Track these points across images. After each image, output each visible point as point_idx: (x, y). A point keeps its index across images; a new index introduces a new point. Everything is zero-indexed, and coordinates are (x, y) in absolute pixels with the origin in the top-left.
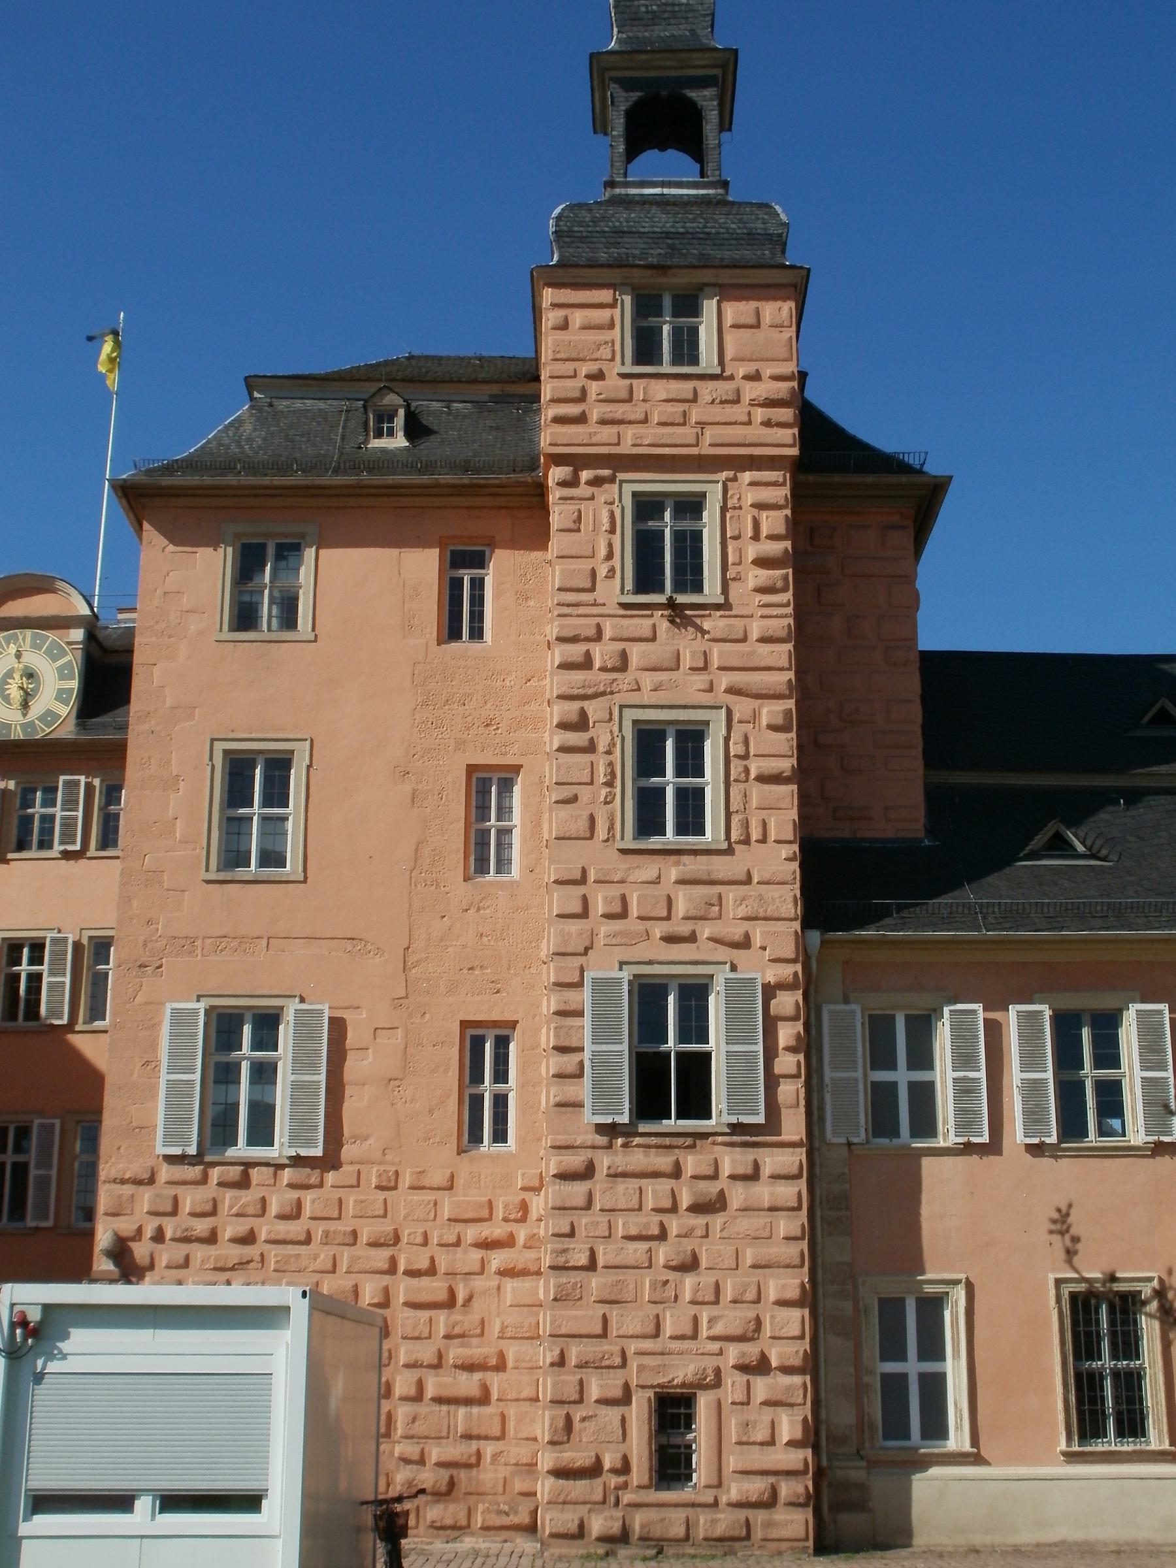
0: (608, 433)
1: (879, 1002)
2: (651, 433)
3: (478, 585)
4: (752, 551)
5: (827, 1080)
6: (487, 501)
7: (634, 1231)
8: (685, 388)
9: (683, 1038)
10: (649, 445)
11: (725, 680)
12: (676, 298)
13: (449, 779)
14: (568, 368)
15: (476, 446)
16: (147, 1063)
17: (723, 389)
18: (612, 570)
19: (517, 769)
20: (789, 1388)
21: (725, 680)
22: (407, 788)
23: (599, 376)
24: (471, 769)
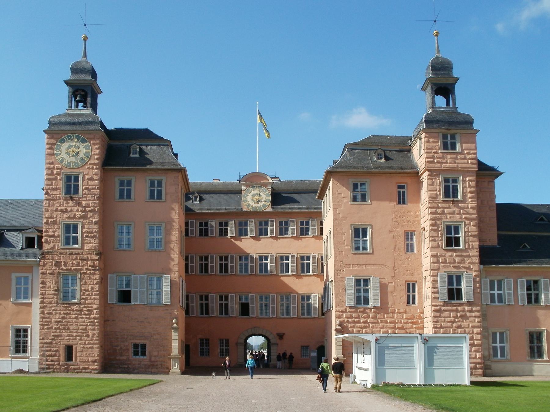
0: (438, 165)
1: (492, 278)
2: (447, 165)
3: (404, 192)
4: (468, 190)
5: (483, 293)
6: (406, 175)
7: (449, 321)
8: (454, 156)
9: (457, 285)
10: (447, 167)
11: (464, 216)
12: (451, 135)
13: (401, 233)
14: (430, 151)
15: (400, 162)
16: (343, 289)
17: (462, 156)
18: (440, 193)
19: (414, 231)
20: (479, 348)
21: (464, 216)
22: (392, 235)
23: (436, 153)
24: (405, 231)
